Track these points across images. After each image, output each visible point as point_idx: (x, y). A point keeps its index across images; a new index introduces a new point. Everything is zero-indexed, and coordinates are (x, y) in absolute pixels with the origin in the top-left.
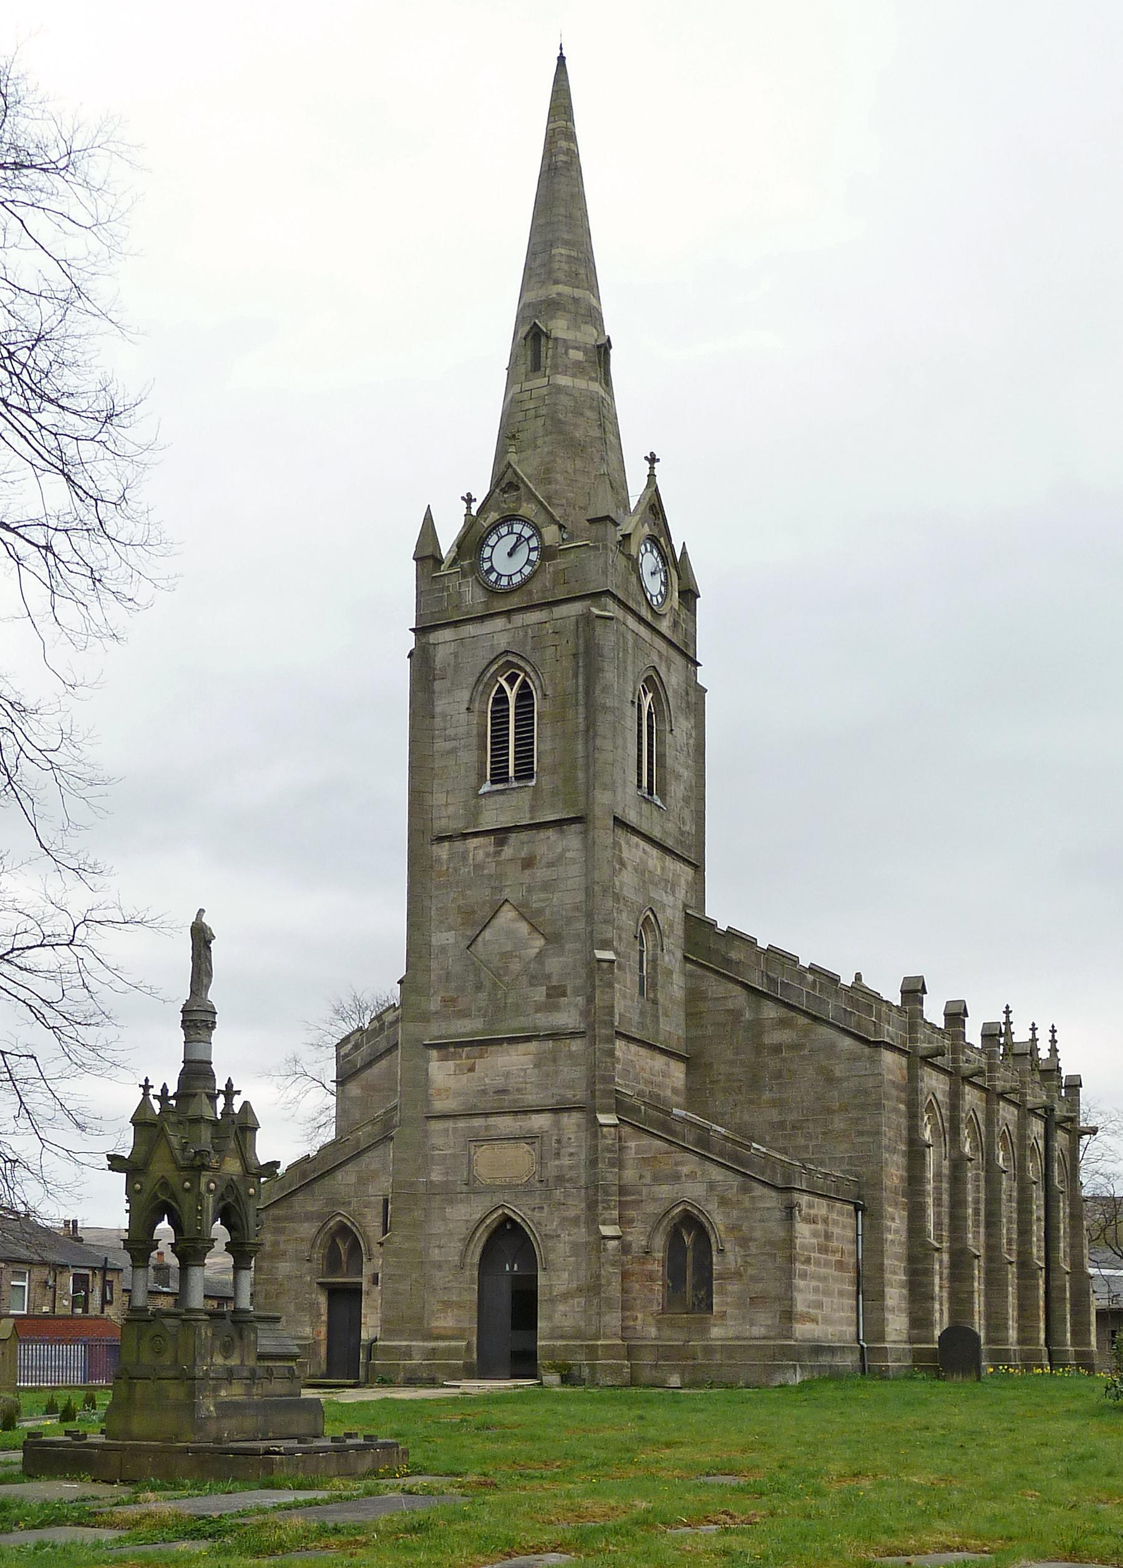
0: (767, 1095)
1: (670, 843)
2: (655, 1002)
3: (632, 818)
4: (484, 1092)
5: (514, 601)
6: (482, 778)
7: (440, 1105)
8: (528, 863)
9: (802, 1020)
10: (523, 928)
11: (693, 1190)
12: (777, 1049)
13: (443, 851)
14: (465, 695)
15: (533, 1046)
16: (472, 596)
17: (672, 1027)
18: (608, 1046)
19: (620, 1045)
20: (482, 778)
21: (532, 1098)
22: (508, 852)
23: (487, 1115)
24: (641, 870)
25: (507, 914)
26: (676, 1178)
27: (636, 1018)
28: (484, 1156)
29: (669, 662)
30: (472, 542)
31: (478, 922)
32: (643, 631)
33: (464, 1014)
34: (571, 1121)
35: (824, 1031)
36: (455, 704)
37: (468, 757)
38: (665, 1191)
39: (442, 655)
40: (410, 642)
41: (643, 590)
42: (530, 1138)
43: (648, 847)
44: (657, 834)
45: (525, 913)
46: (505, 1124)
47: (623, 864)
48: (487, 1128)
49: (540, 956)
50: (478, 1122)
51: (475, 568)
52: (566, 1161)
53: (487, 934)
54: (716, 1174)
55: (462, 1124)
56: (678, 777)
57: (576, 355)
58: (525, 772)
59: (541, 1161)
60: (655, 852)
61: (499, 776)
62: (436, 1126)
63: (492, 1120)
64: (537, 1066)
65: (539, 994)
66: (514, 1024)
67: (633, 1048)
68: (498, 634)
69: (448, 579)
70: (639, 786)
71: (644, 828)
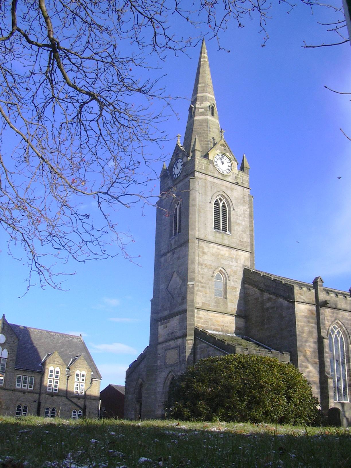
0: (266, 326)
1: (233, 246)
2: (226, 298)
4: (168, 334)
5: (178, 181)
9: (274, 297)
10: (178, 279)
12: (267, 309)
13: (162, 260)
15: (178, 317)
18: (191, 313)
19: (202, 313)
22: (175, 256)
25: (175, 275)
27: (213, 304)
33: (165, 310)
35: (280, 300)
37: (168, 230)
43: (220, 247)
44: (226, 242)
48: (169, 346)
50: (167, 344)
56: (239, 224)
60: (225, 249)
61: (175, 234)
64: (180, 323)
67: (211, 314)
70: (217, 227)
71: (218, 241)
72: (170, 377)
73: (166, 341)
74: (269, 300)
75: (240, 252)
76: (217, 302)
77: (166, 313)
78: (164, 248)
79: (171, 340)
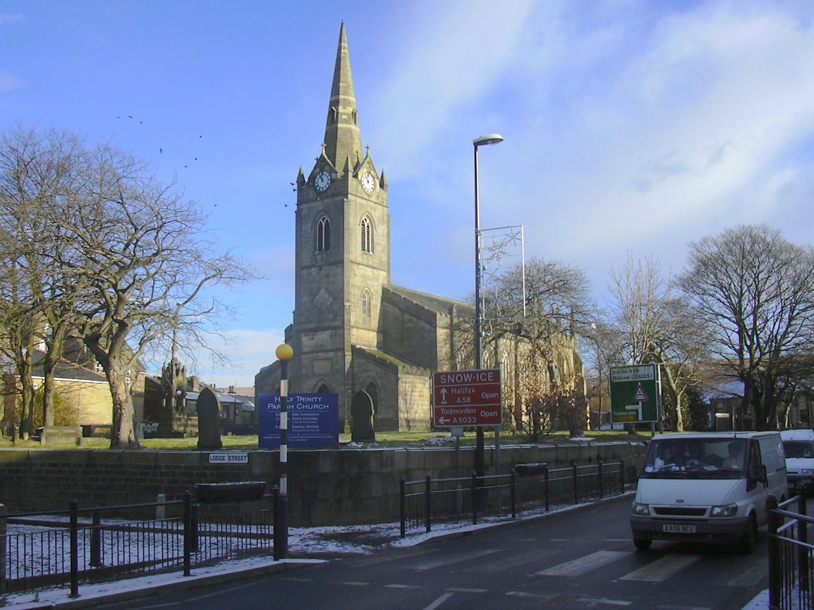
1: (376, 266)
3: (359, 260)
6: (315, 250)
7: (305, 350)
8: (328, 276)
9: (415, 320)
10: (327, 296)
11: (373, 374)
13: (305, 272)
14: (311, 224)
15: (328, 332)
16: (312, 194)
17: (375, 323)
20: (315, 250)
21: (329, 347)
23: (317, 352)
24: (364, 277)
25: (322, 291)
26: (367, 371)
27: (361, 322)
28: (316, 364)
29: (375, 209)
30: (313, 177)
31: (314, 293)
32: (364, 202)
33: (311, 322)
34: (340, 354)
35: (422, 323)
36: (307, 227)
37: (311, 243)
38: (365, 375)
39: (304, 212)
40: (295, 208)
41: (364, 190)
42: (328, 359)
43: (366, 268)
44: (370, 263)
45: (327, 289)
46: (321, 355)
47: (355, 275)
49: (332, 304)
50: (315, 355)
51: (314, 185)
52: (338, 367)
53: (317, 297)
54: (378, 370)
55: (311, 355)
56: (379, 244)
57: (345, 117)
58: (327, 247)
59: (332, 367)
60: (370, 269)
62: (304, 356)
63: (319, 354)
65: (331, 316)
66: (325, 325)
67: (360, 331)
68: (318, 205)
69: (305, 187)
70: (363, 249)
71: (365, 262)
72: (320, 385)
73: (313, 352)
74: (410, 321)
75: (380, 272)
76: (364, 320)
77: (311, 326)
78: (307, 261)
79: (321, 351)
